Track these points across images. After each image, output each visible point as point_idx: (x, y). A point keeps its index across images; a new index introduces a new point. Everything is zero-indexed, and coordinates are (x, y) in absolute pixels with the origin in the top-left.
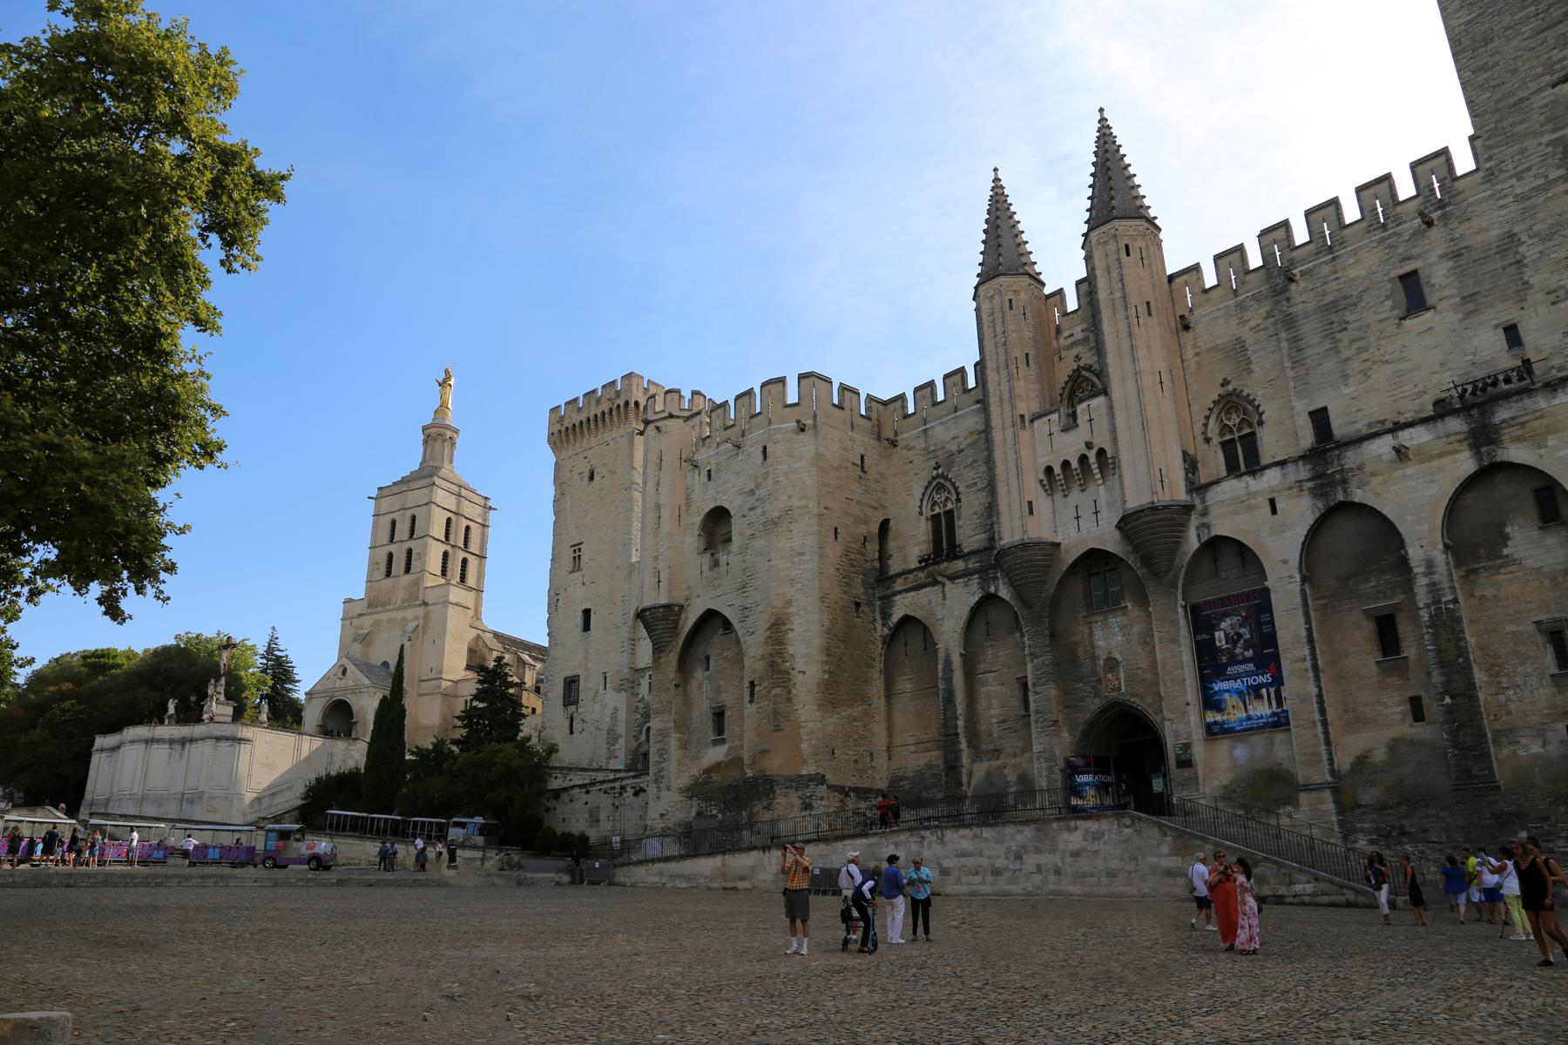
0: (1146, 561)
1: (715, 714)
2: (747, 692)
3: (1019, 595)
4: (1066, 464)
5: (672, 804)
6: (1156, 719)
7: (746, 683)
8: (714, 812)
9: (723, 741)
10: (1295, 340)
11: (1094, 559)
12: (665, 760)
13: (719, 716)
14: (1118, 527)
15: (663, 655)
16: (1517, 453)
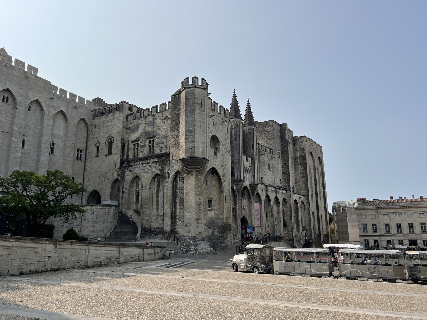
0: (252, 192)
1: (209, 201)
2: (224, 198)
3: (237, 190)
4: (246, 167)
5: (203, 229)
6: (248, 221)
7: (224, 196)
8: (217, 233)
9: (212, 210)
10: (261, 165)
11: (246, 187)
12: (200, 213)
13: (210, 201)
14: (250, 185)
15: (199, 175)
16: (278, 196)
